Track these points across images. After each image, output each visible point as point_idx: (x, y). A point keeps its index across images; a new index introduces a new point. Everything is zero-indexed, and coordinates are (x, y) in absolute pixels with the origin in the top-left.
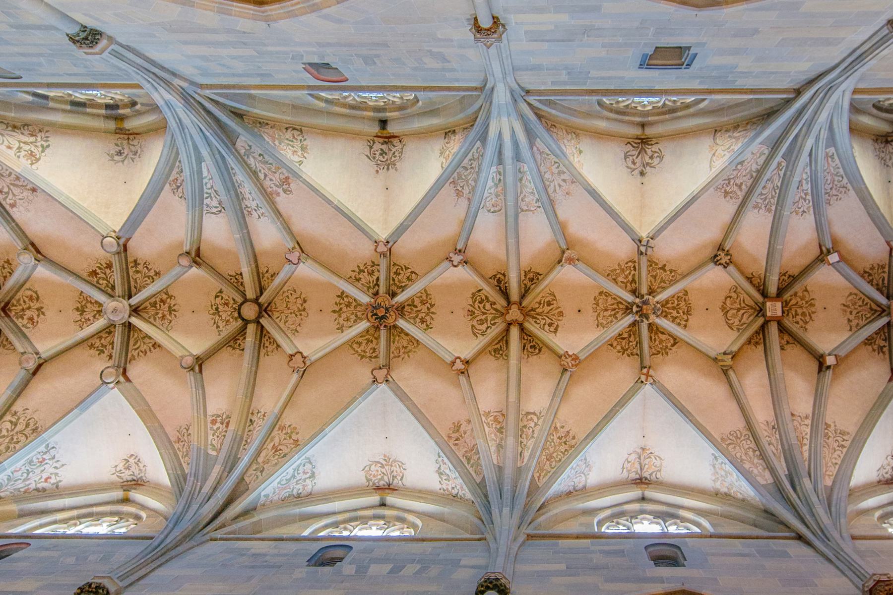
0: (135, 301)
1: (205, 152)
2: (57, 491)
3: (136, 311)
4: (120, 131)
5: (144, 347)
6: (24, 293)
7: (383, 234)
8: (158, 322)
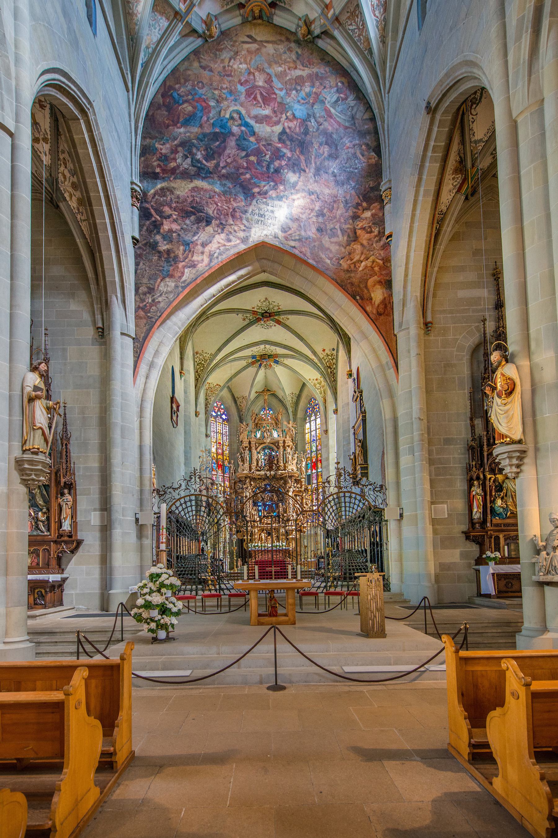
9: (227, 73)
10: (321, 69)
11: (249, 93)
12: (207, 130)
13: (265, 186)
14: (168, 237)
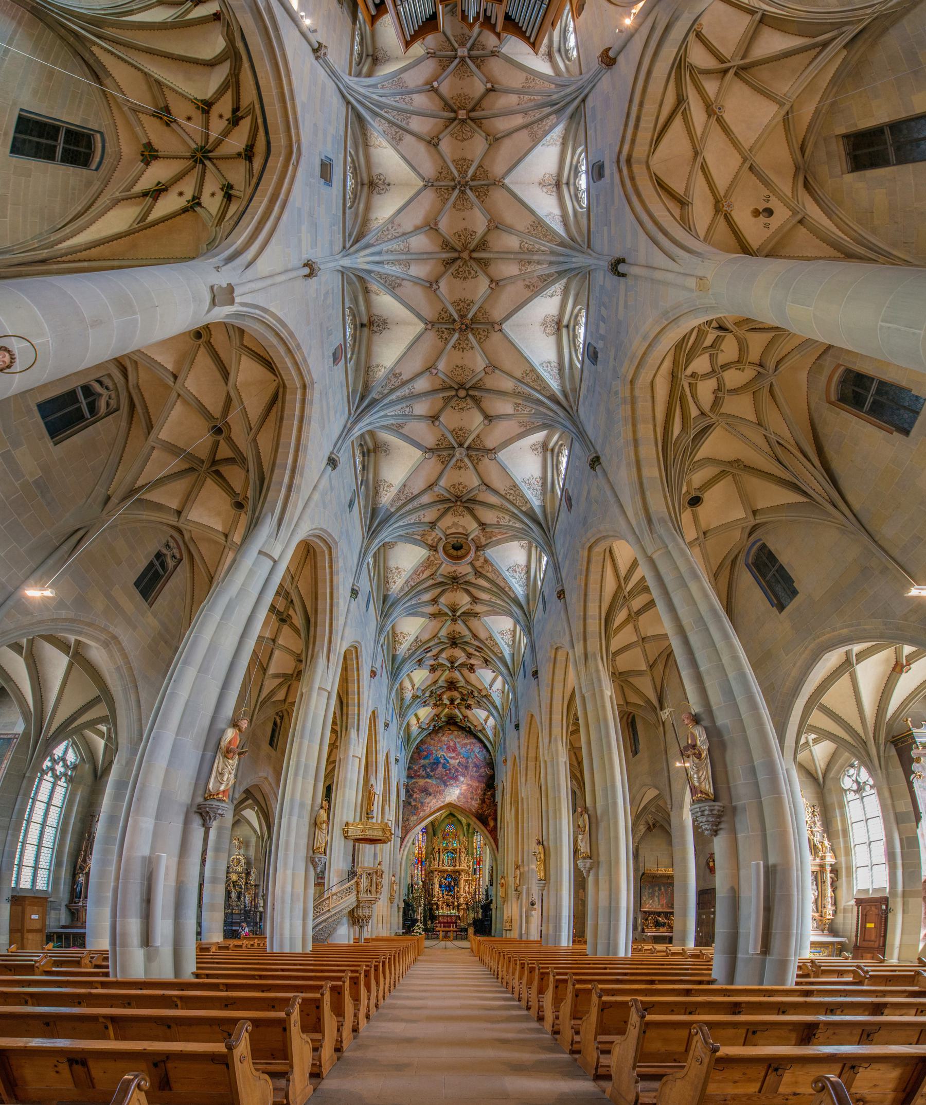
0: (456, 446)
1: (382, 413)
2: (544, 478)
3: (461, 445)
4: (375, 452)
5: (479, 442)
6: (452, 490)
7: (421, 326)
8: (467, 435)
9: (440, 741)
10: (474, 741)
11: (448, 748)
12: (432, 761)
13: (452, 782)
14: (415, 800)
